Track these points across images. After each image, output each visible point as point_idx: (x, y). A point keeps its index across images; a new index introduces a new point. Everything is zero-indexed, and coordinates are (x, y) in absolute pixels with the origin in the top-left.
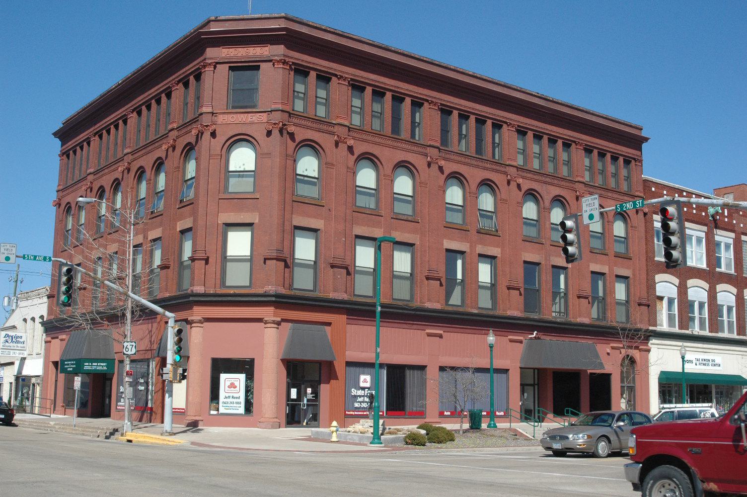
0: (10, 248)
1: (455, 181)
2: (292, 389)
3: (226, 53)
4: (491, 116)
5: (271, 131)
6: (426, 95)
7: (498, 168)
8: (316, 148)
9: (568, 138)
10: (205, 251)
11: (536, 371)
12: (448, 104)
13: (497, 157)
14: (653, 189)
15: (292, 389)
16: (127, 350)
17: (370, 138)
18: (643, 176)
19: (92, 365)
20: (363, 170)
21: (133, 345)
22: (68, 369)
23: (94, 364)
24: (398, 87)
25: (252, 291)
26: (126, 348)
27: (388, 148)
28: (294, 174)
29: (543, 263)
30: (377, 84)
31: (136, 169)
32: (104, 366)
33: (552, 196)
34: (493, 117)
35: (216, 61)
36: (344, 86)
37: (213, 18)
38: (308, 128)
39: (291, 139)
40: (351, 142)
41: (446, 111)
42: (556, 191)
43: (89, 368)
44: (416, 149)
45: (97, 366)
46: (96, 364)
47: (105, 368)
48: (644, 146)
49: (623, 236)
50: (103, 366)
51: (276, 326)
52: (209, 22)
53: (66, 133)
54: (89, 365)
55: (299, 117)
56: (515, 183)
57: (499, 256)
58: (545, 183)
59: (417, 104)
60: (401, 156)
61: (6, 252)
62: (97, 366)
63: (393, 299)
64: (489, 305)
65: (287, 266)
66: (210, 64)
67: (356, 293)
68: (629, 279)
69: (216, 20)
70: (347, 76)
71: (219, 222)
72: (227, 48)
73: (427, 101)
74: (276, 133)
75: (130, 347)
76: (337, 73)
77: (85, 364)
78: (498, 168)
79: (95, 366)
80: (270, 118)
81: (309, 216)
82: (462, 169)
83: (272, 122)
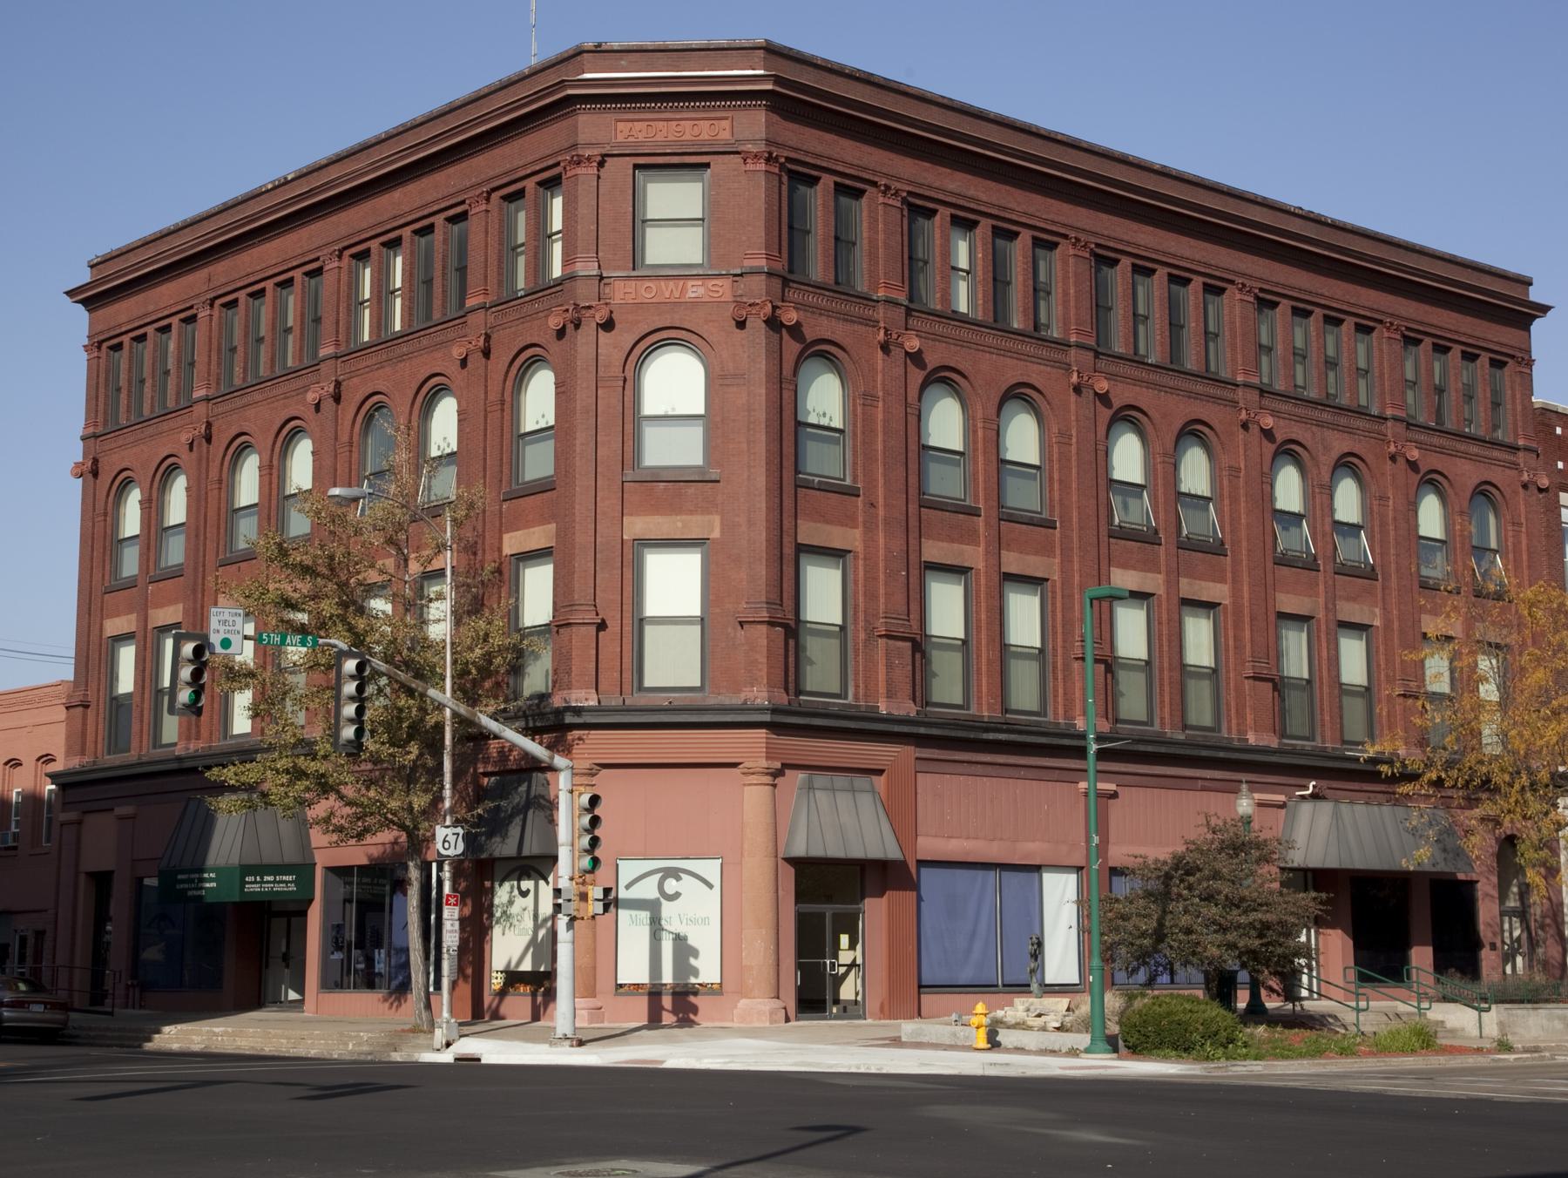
0: (231, 619)
1: (1429, 487)
2: (842, 936)
3: (626, 132)
4: (1203, 270)
5: (745, 321)
6: (1064, 225)
7: (1219, 392)
8: (952, 380)
9: (1369, 314)
10: (595, 606)
11: (1310, 875)
12: (1111, 244)
13: (1213, 368)
14: (1559, 431)
15: (842, 936)
16: (446, 845)
17: (1474, 449)
18: (1534, 400)
19: (262, 882)
20: (1013, 422)
21: (458, 834)
22: (190, 893)
23: (266, 878)
24: (1005, 208)
25: (712, 701)
26: (444, 841)
27: (944, 345)
28: (1102, 482)
29: (1321, 615)
30: (961, 202)
31: (359, 397)
32: (290, 882)
33: (1335, 454)
34: (1207, 271)
35: (604, 151)
36: (894, 210)
37: (590, 45)
38: (1197, 396)
39: (1412, 470)
40: (1268, 422)
41: (1104, 259)
42: (1340, 444)
43: (256, 888)
44: (1045, 353)
45: (274, 882)
46: (270, 878)
47: (292, 888)
48: (1537, 326)
49: (1438, 536)
50: (286, 882)
51: (768, 779)
52: (579, 52)
53: (92, 298)
54: (255, 882)
55: (802, 287)
56: (1091, 392)
57: (1226, 602)
58: (1321, 424)
59: (849, 189)
60: (1014, 372)
61: (222, 628)
62: (274, 882)
63: (1344, 742)
64: (1207, 720)
65: (1275, 688)
66: (589, 159)
67: (1346, 738)
68: (1370, 630)
69: (598, 50)
70: (899, 186)
71: (625, 537)
72: (628, 121)
73: (1513, 357)
74: (756, 325)
75: (452, 839)
76: (876, 179)
77: (215, 885)
78: (1219, 392)
79: (268, 882)
80: (740, 292)
81: (827, 522)
82: (1143, 397)
83: (745, 300)
